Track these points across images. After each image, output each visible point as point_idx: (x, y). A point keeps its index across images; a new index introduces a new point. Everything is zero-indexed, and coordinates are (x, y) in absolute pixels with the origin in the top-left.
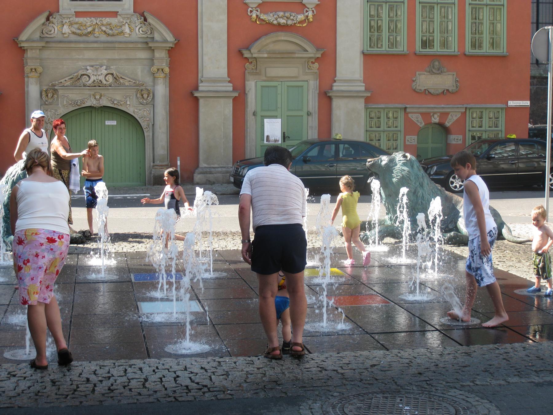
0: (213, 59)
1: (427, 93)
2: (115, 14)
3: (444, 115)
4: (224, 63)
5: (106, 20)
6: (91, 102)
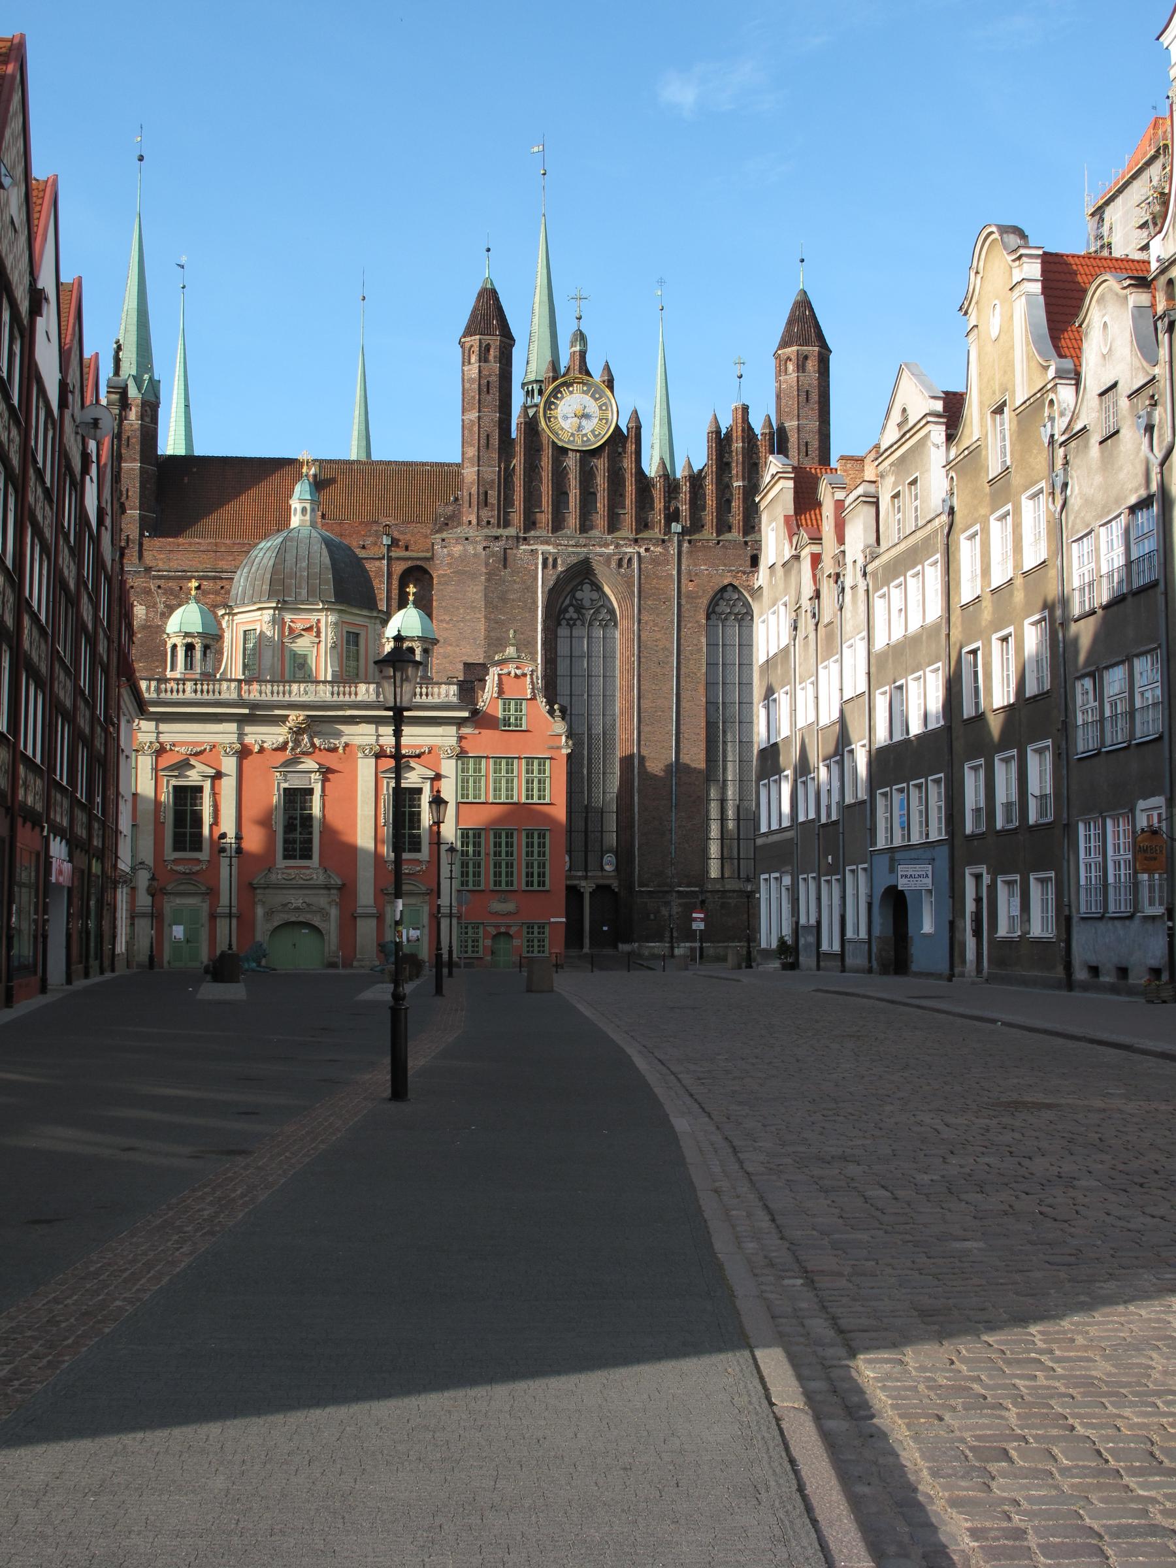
0: (366, 894)
1: (496, 914)
2: (308, 868)
3: (509, 926)
4: (372, 896)
5: (303, 871)
6: (293, 919)
